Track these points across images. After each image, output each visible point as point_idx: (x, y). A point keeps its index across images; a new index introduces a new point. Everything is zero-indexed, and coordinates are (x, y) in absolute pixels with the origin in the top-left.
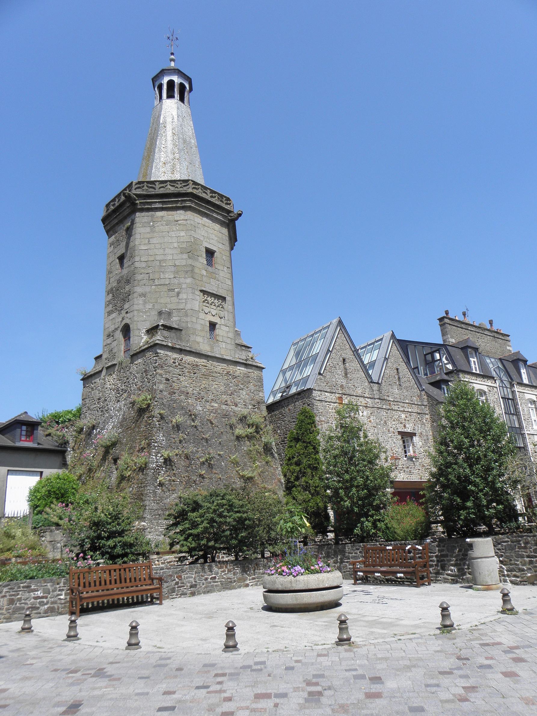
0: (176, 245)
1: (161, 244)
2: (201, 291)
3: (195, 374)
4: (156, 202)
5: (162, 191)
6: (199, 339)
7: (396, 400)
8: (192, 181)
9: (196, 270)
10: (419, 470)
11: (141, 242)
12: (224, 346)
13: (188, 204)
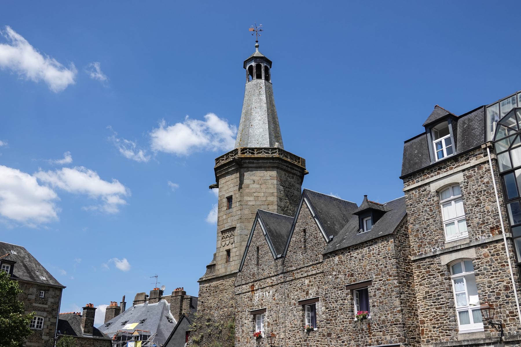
7: (298, 267)
10: (318, 341)
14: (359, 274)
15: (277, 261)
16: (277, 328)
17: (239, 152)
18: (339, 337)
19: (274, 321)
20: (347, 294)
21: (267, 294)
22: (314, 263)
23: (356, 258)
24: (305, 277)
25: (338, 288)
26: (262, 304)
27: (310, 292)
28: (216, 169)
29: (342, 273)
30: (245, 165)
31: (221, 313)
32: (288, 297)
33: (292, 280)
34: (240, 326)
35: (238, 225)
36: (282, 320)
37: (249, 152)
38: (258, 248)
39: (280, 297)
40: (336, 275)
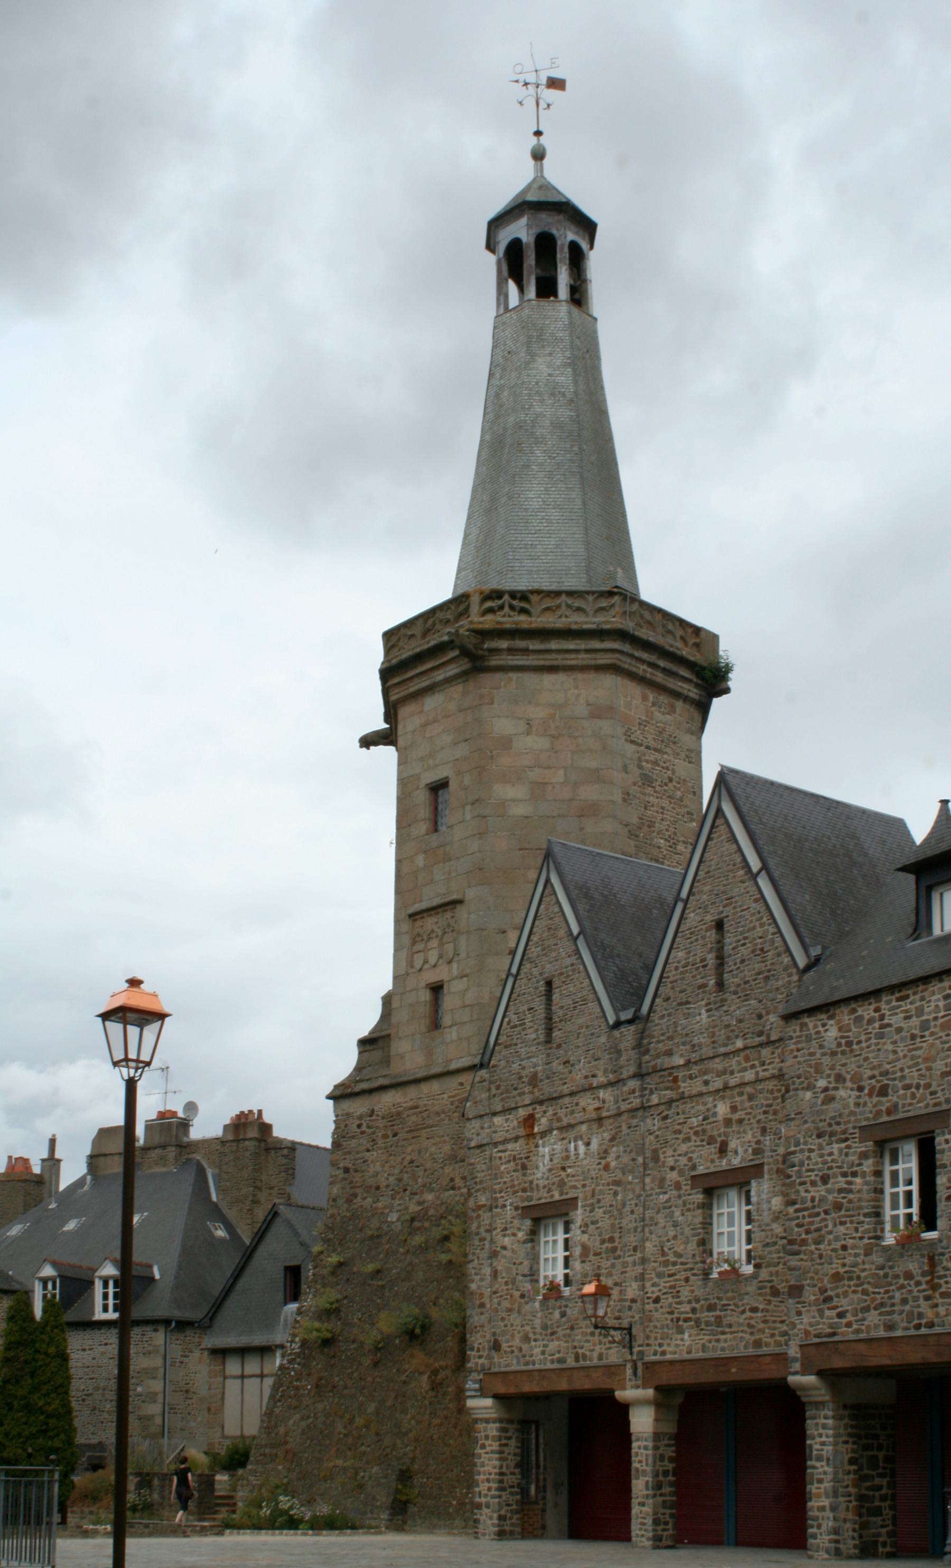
7: (694, 1056)
14: (907, 1087)
15: (616, 1033)
16: (613, 1265)
17: (475, 609)
18: (828, 1299)
19: (603, 1242)
20: (864, 1156)
21: (582, 1149)
22: (749, 1042)
23: (899, 1030)
24: (718, 1091)
25: (832, 1134)
26: (562, 1184)
27: (732, 1145)
28: (386, 674)
29: (849, 1084)
30: (494, 661)
31: (414, 1208)
32: (656, 1159)
33: (670, 1102)
34: (484, 1254)
35: (471, 894)
36: (632, 1239)
37: (512, 608)
38: (549, 984)
39: (626, 1159)
40: (826, 1089)
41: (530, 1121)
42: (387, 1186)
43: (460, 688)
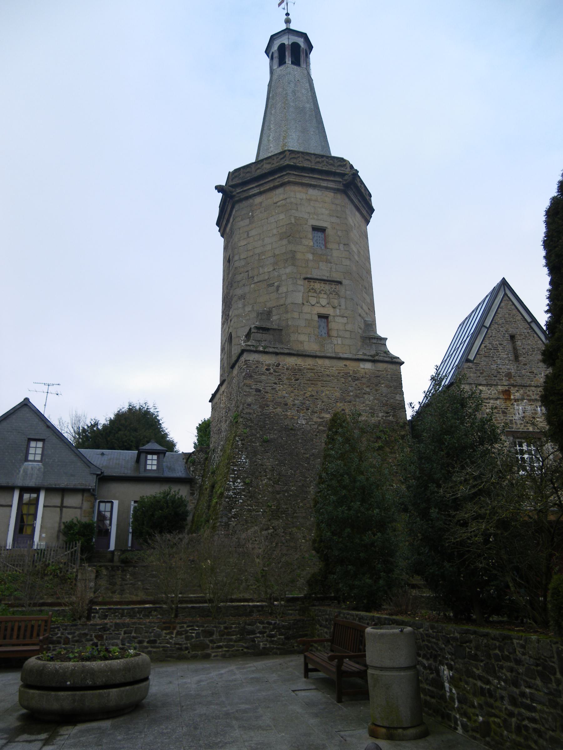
0: (275, 231)
1: (260, 234)
2: (305, 279)
3: (297, 380)
4: (253, 188)
5: (259, 172)
6: (302, 338)
8: (289, 151)
9: (299, 256)
11: (241, 237)
12: (340, 342)
13: (286, 179)
41: (507, 393)
42: (294, 405)
43: (332, 194)
